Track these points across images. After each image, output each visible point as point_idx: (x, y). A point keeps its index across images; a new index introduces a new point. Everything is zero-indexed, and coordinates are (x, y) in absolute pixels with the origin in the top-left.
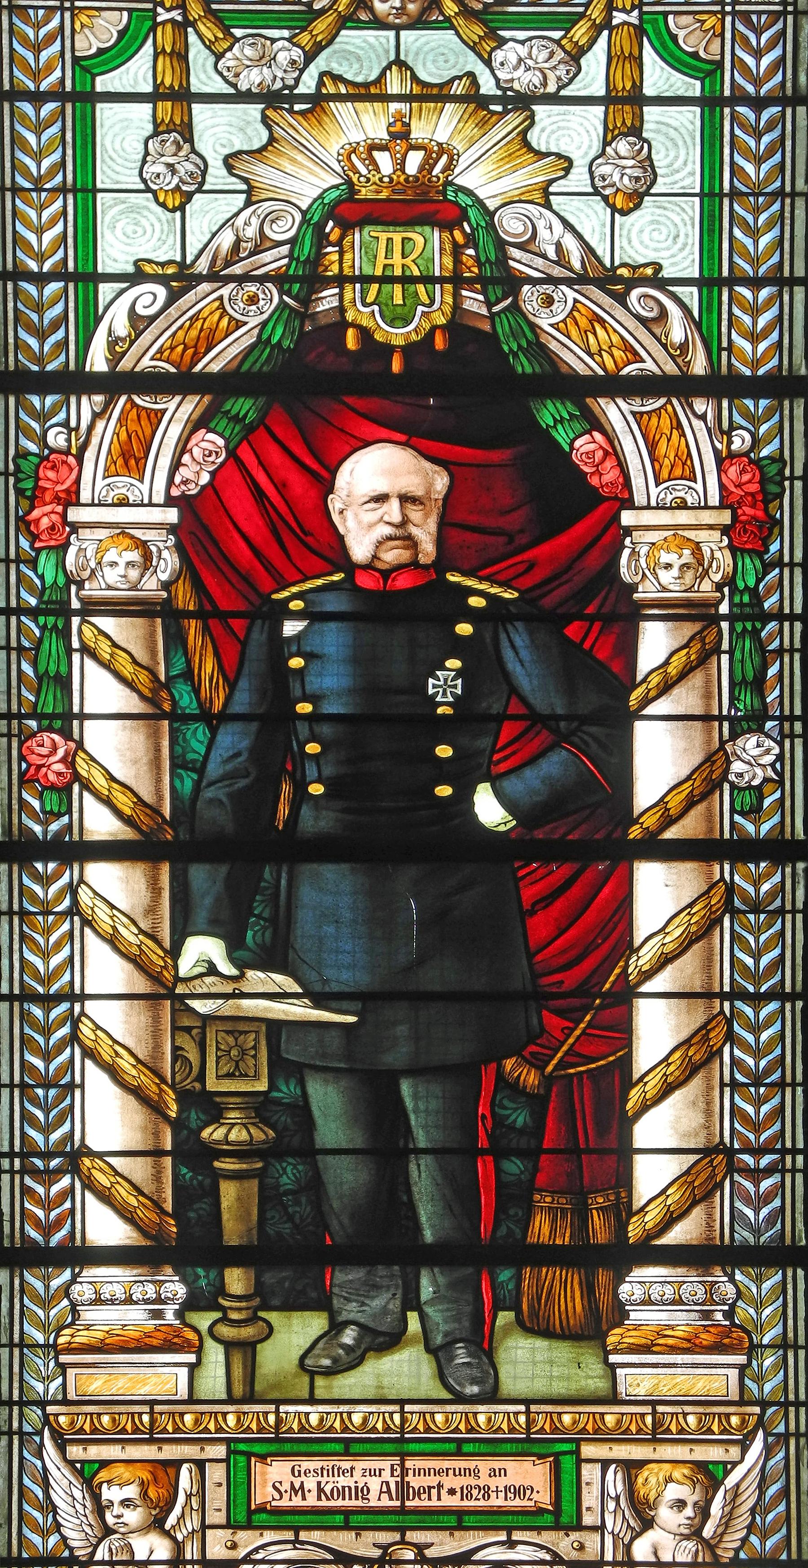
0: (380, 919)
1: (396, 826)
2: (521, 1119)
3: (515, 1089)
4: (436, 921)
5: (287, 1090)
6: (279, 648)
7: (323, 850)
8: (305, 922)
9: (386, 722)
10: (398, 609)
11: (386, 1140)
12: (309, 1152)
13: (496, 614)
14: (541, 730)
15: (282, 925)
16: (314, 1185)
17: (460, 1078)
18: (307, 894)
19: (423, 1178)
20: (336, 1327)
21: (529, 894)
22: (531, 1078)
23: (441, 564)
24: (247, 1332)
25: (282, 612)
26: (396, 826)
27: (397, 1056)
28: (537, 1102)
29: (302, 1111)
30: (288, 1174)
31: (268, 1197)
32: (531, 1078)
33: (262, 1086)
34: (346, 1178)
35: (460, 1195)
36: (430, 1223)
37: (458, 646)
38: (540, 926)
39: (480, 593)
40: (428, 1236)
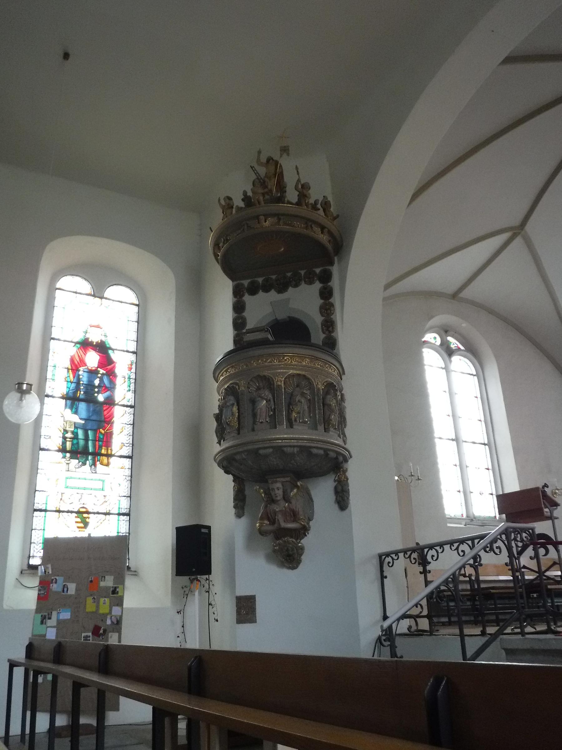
0: (88, 410)
1: (90, 399)
2: (102, 437)
3: (101, 433)
4: (94, 411)
5: (76, 431)
6: (79, 375)
7: (82, 400)
8: (80, 409)
9: (90, 386)
10: (92, 373)
11: (86, 439)
12: (77, 439)
13: (103, 374)
14: (106, 389)
15: (77, 409)
16: (78, 443)
17: (96, 431)
18: (80, 405)
19: (90, 443)
20: (79, 462)
21: (105, 408)
22: (103, 432)
23: (98, 368)
24: (68, 462)
25: (79, 371)
26: (90, 399)
27: (88, 428)
28: (104, 435)
29: (77, 433)
30: (75, 441)
31: (73, 444)
32: (103, 432)
33: (73, 429)
34: (82, 443)
35: (94, 446)
36: (91, 449)
37: (99, 377)
38: (106, 412)
39: (102, 371)
40: (90, 451)
